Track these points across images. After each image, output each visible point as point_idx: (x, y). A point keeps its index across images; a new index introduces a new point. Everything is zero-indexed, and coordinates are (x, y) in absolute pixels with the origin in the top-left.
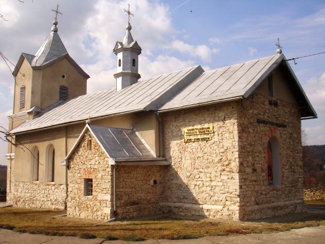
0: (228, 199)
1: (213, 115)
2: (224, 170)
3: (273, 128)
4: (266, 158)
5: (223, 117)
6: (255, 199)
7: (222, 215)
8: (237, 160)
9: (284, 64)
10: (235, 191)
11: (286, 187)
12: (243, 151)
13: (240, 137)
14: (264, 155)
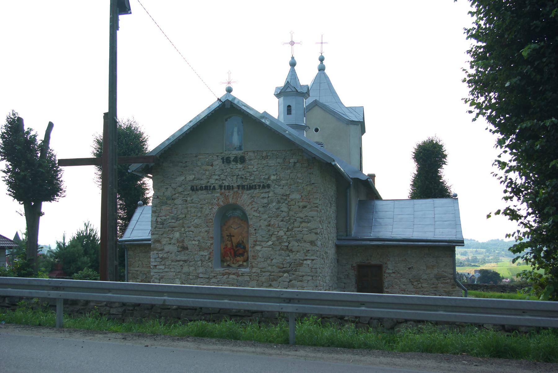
3: (230, 194)
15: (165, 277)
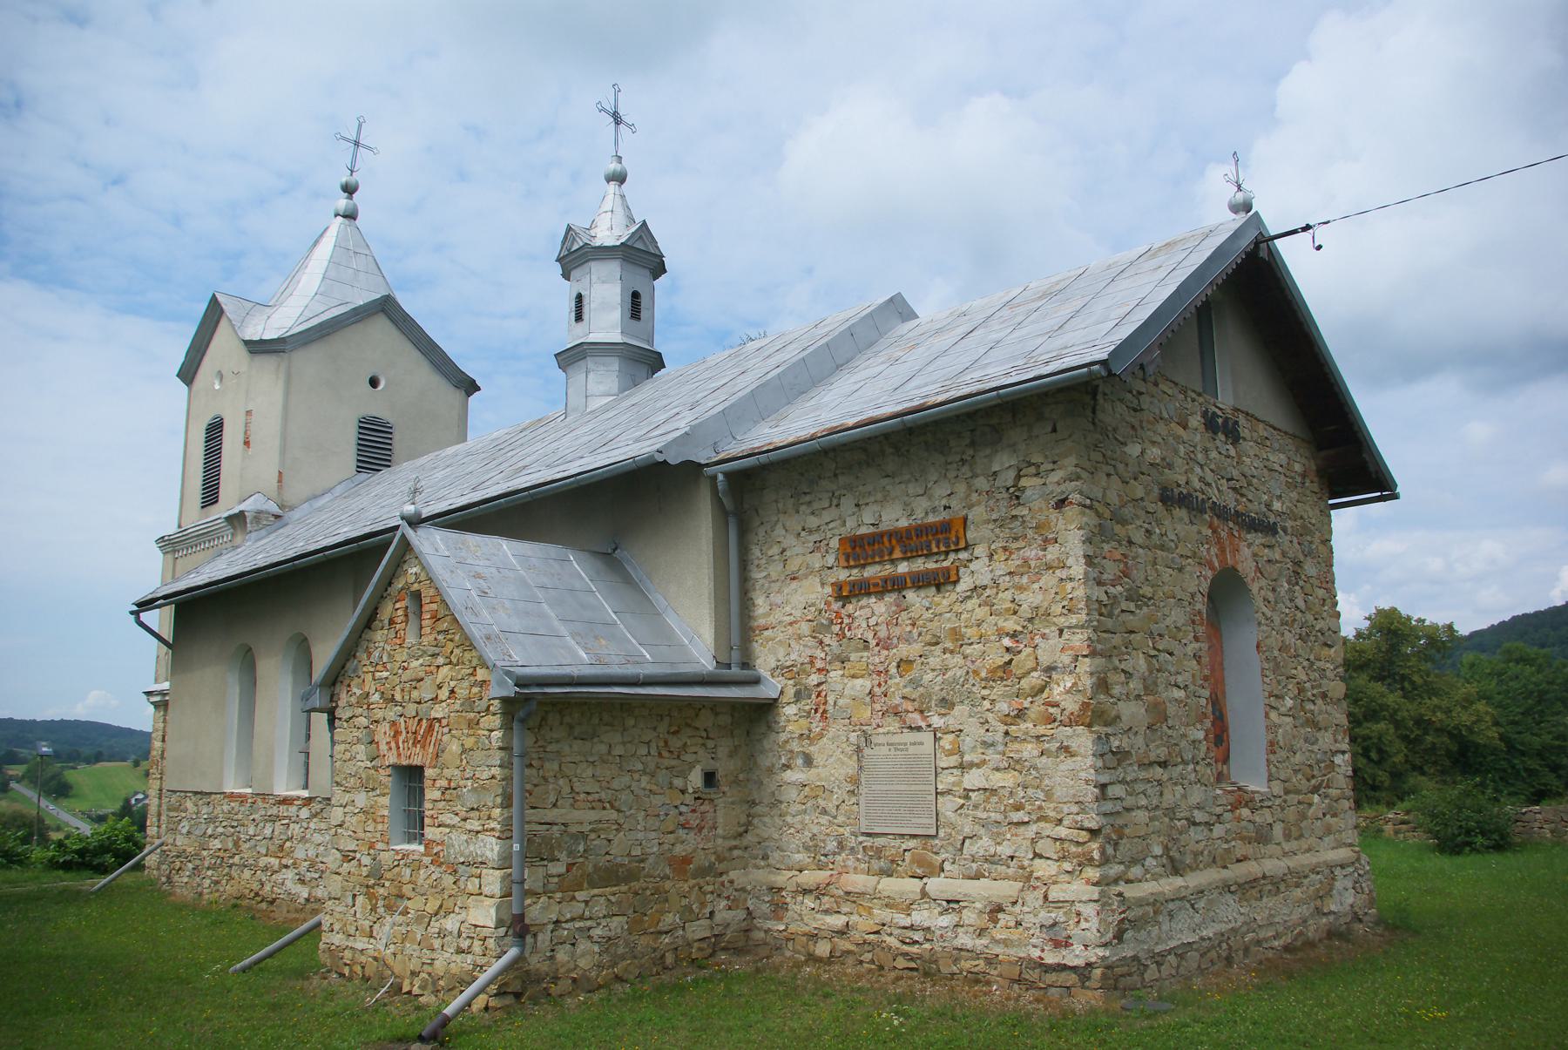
0: (1044, 846)
1: (965, 469)
2: (1021, 714)
4: (1205, 660)
5: (1012, 474)
6: (1166, 848)
7: (1019, 924)
8: (1085, 665)
9: (1263, 254)
10: (1075, 809)
11: (1287, 792)
12: (1109, 623)
13: (1089, 560)
14: (1193, 647)
15: (1127, 831)
